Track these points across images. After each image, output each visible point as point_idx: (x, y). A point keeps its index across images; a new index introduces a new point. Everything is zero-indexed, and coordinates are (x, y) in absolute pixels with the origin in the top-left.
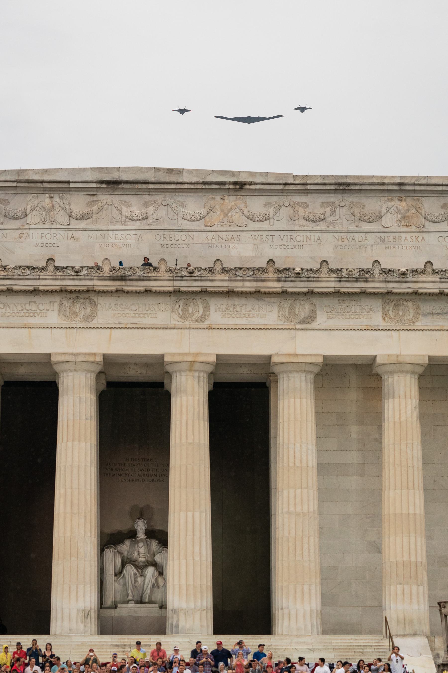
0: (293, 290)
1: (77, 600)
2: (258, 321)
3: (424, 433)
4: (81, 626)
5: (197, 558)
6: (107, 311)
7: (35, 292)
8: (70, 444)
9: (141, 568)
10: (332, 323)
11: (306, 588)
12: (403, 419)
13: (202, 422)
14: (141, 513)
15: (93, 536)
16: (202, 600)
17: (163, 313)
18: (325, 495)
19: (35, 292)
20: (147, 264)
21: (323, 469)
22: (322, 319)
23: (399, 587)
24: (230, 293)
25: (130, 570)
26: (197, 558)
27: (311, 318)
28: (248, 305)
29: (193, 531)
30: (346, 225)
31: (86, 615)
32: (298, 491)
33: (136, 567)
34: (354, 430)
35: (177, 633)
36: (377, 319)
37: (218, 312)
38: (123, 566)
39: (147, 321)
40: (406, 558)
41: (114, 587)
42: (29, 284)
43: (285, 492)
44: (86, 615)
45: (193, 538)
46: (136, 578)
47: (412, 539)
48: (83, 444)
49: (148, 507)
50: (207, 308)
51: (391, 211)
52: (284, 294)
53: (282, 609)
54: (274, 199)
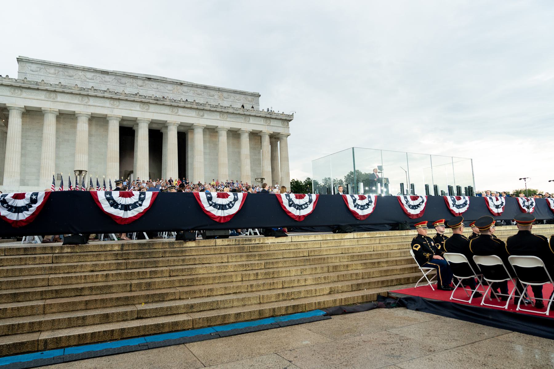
0: (200, 109)
2: (190, 115)
6: (152, 108)
7: (134, 101)
10: (208, 117)
17: (167, 110)
19: (134, 101)
20: (164, 97)
22: (206, 116)
24: (184, 107)
27: (203, 115)
28: (188, 111)
30: (206, 97)
36: (218, 117)
37: (181, 111)
39: (162, 112)
42: (132, 99)
50: (178, 110)
51: (216, 94)
52: (197, 109)
54: (189, 88)
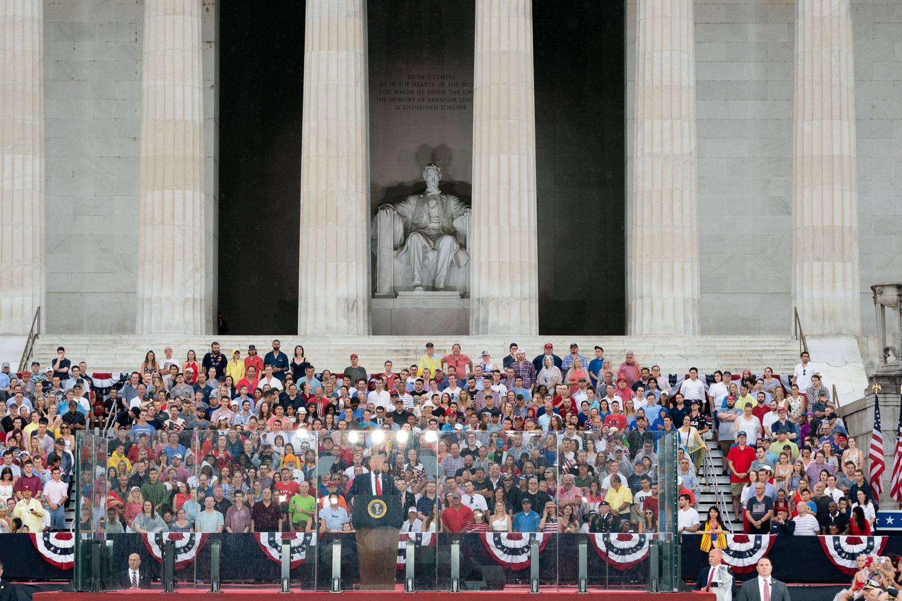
1: (337, 285)
3: (857, 35)
4: (343, 323)
5: (515, 223)
8: (324, 53)
9: (433, 238)
11: (677, 267)
12: (826, 13)
13: (522, 20)
14: (434, 157)
15: (360, 190)
16: (522, 284)
18: (707, 129)
21: (703, 89)
23: (816, 264)
25: (416, 241)
26: (515, 223)
29: (509, 184)
31: (351, 306)
32: (667, 123)
33: (426, 236)
34: (752, 31)
35: (486, 332)
38: (406, 235)
40: (827, 222)
41: (392, 268)
43: (647, 124)
44: (351, 306)
45: (509, 193)
46: (425, 253)
47: (837, 193)
48: (343, 53)
49: (443, 148)
53: (642, 297)
